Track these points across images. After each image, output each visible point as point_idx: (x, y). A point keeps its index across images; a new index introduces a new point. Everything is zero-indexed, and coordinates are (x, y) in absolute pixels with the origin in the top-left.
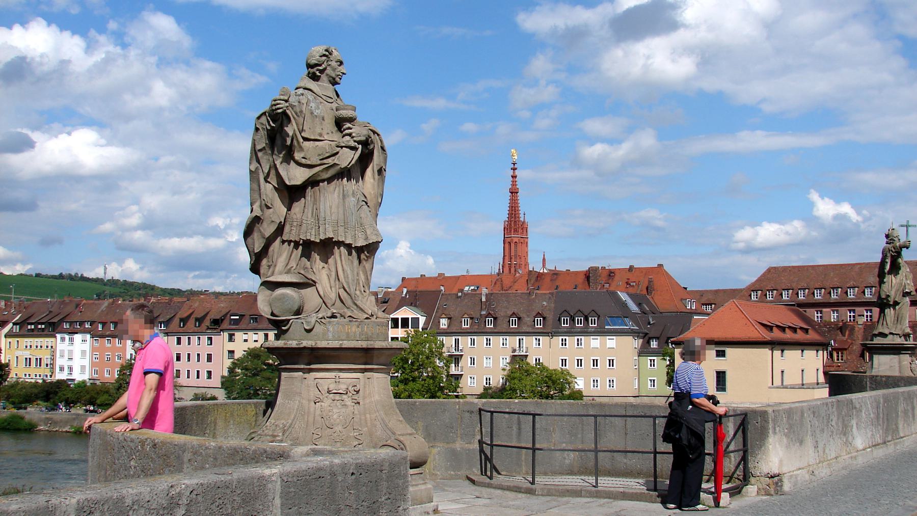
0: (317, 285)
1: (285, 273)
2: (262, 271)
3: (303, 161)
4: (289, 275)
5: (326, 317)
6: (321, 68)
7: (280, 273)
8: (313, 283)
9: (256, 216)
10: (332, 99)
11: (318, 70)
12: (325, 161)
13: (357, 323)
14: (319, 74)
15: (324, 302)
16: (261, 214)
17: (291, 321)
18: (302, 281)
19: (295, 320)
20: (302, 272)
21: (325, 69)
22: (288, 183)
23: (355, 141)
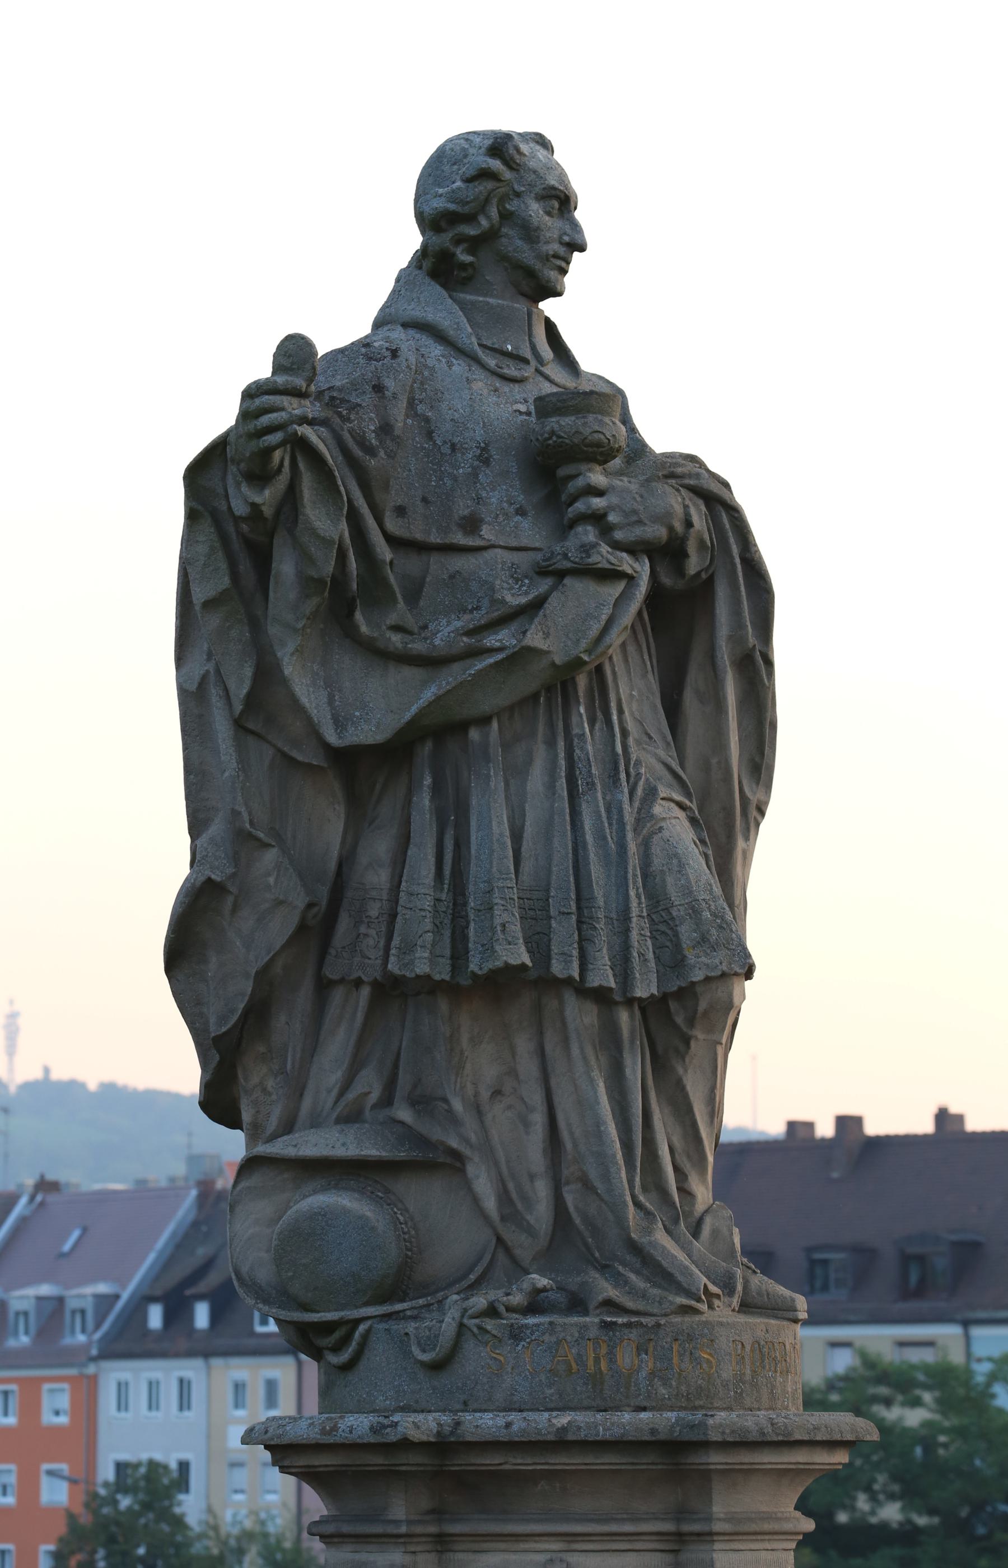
0: (471, 1170)
1: (338, 1121)
2: (246, 1117)
3: (396, 639)
4: (352, 1131)
5: (502, 1309)
6: (471, 231)
7: (315, 1123)
8: (448, 1160)
9: (209, 880)
10: (526, 361)
11: (458, 240)
12: (491, 641)
13: (634, 1334)
14: (467, 258)
15: (500, 1240)
16: (230, 870)
17: (362, 1328)
18: (402, 1155)
19: (382, 1326)
20: (404, 1114)
21: (490, 236)
22: (332, 738)
23: (617, 546)
